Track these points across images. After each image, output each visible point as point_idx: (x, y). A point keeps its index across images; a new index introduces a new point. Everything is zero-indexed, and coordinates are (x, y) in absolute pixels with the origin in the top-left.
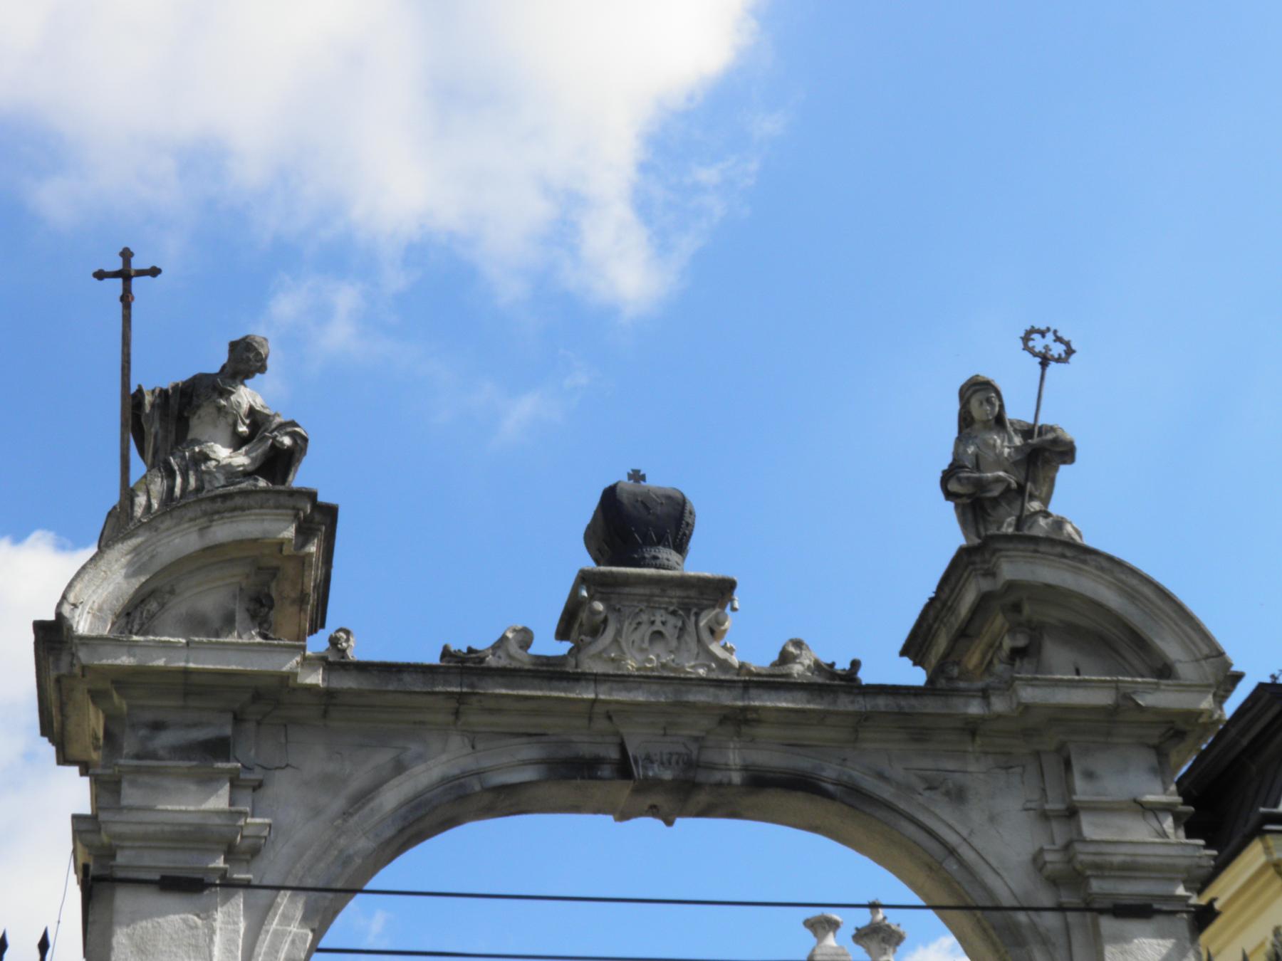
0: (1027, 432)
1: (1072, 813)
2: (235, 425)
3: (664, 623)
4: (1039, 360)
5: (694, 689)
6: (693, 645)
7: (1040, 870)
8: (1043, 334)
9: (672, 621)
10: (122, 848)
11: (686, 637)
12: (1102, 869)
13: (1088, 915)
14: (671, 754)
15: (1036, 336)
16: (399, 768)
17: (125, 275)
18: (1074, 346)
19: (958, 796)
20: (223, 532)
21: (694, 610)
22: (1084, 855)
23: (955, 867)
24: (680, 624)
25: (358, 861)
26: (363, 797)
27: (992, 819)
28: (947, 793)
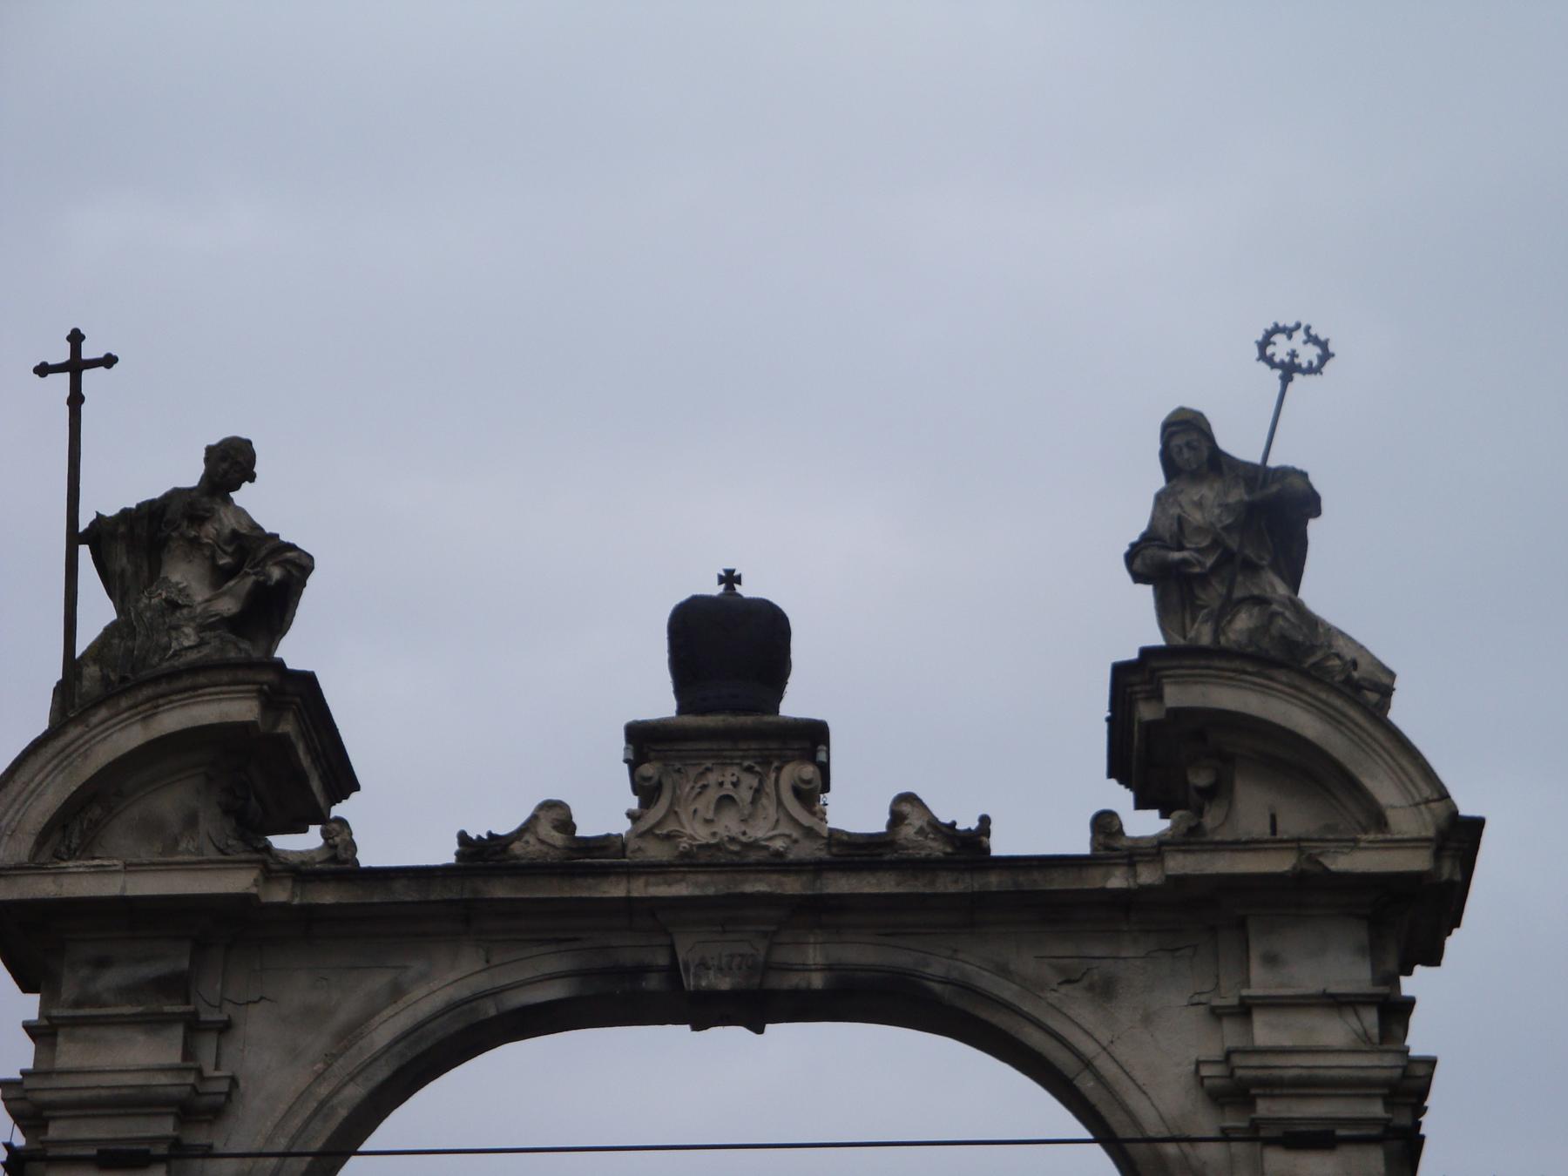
0: (1256, 475)
1: (1244, 1010)
2: (213, 558)
3: (735, 785)
4: (1278, 372)
5: (752, 877)
6: (772, 811)
7: (1202, 1084)
8: (1289, 332)
9: (750, 781)
10: (54, 1118)
11: (764, 801)
12: (1276, 1087)
13: (1258, 1145)
14: (732, 956)
15: (1279, 339)
16: (397, 992)
17: (75, 366)
18: (1331, 348)
19: (1105, 991)
20: (172, 720)
21: (776, 764)
22: (1247, 1067)
23: (1091, 1084)
24: (755, 783)
25: (343, 1113)
26: (350, 1034)
27: (1147, 1020)
28: (1091, 988)
